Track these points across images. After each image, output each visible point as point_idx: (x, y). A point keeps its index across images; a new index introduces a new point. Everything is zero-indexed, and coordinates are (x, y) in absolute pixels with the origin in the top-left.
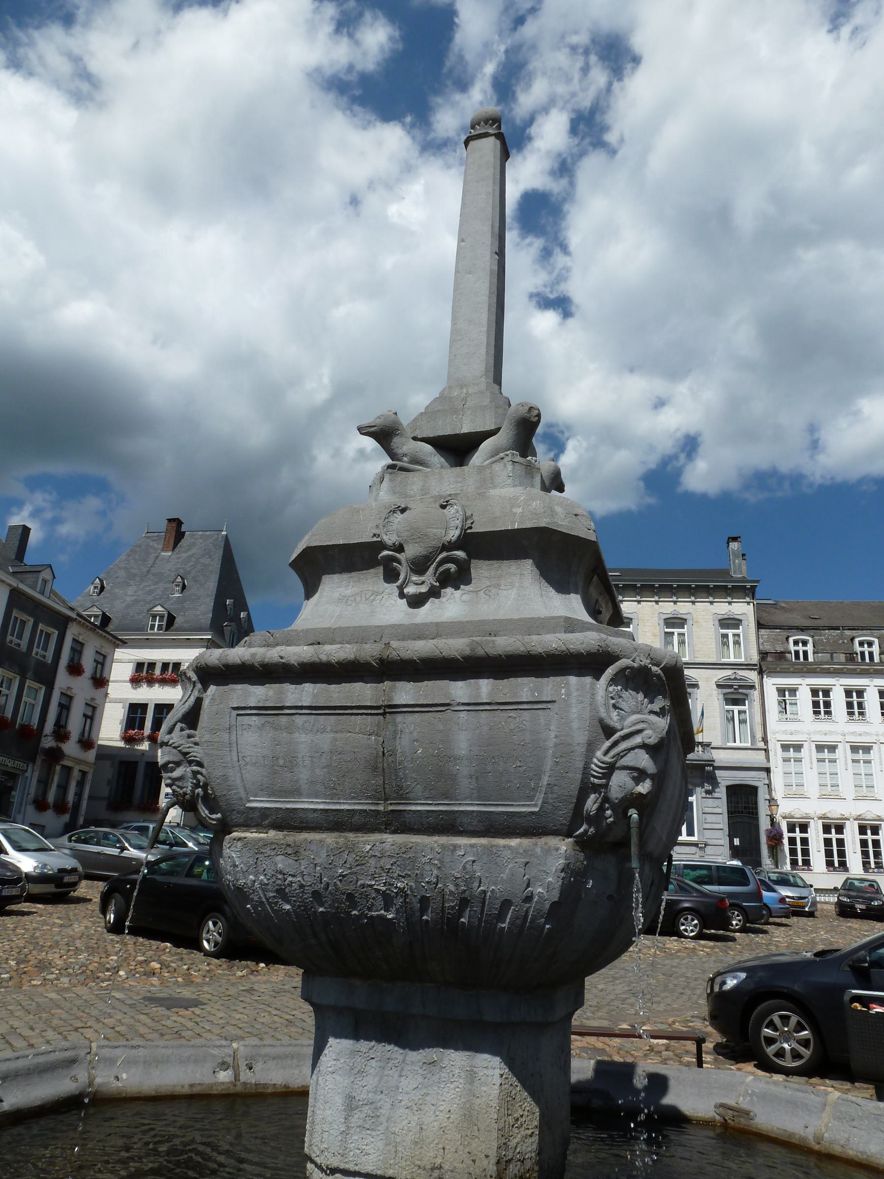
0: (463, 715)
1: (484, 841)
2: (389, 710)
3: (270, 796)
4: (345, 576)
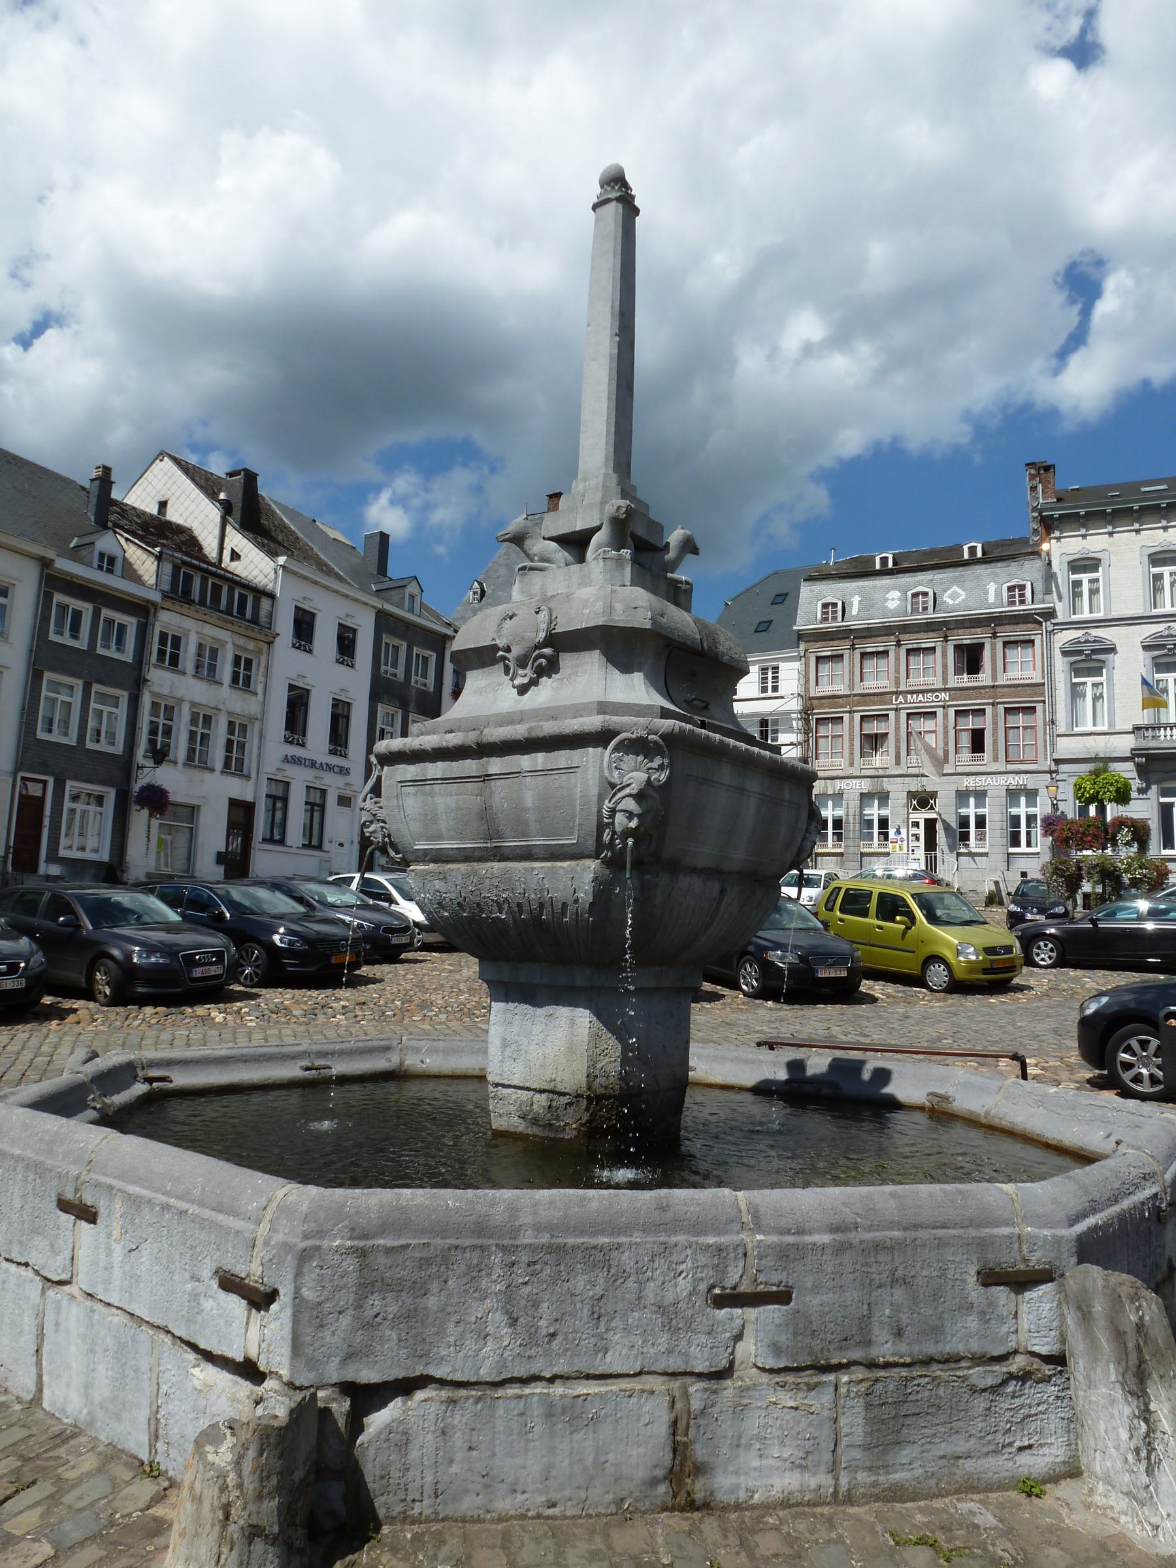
1: (549, 864)
2: (486, 778)
4: (480, 671)
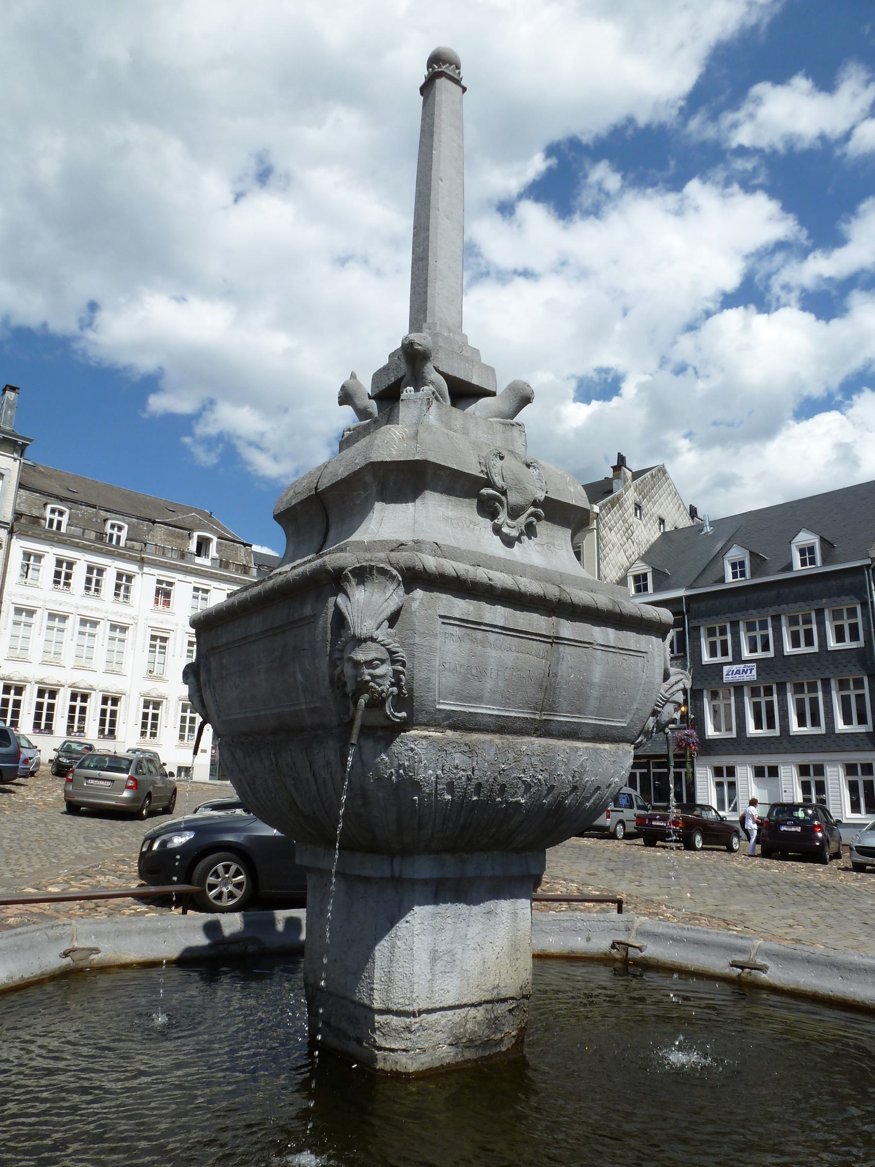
0: (599, 652)
1: (590, 745)
2: (556, 640)
3: (457, 700)
4: (444, 497)
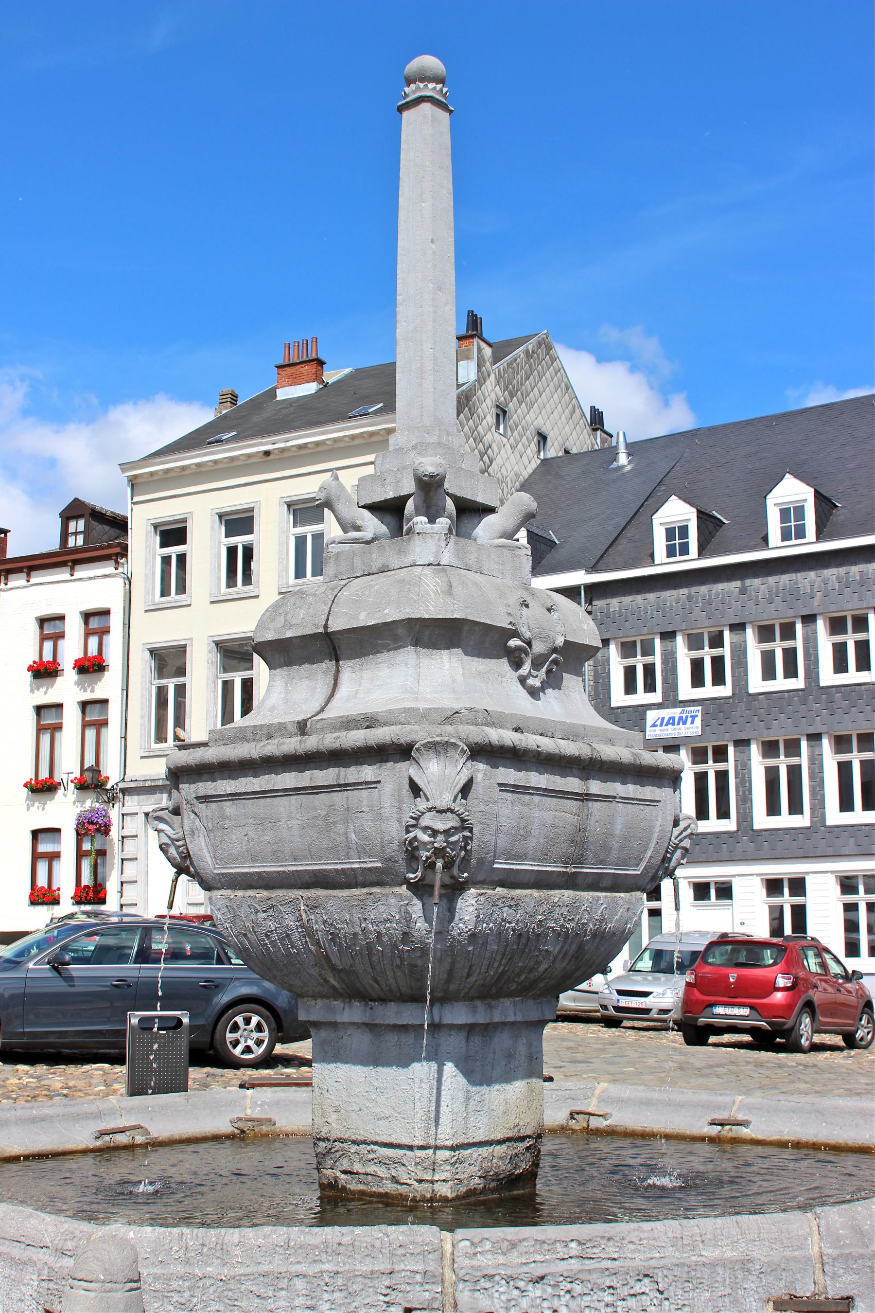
0: (620, 805)
2: (585, 797)
